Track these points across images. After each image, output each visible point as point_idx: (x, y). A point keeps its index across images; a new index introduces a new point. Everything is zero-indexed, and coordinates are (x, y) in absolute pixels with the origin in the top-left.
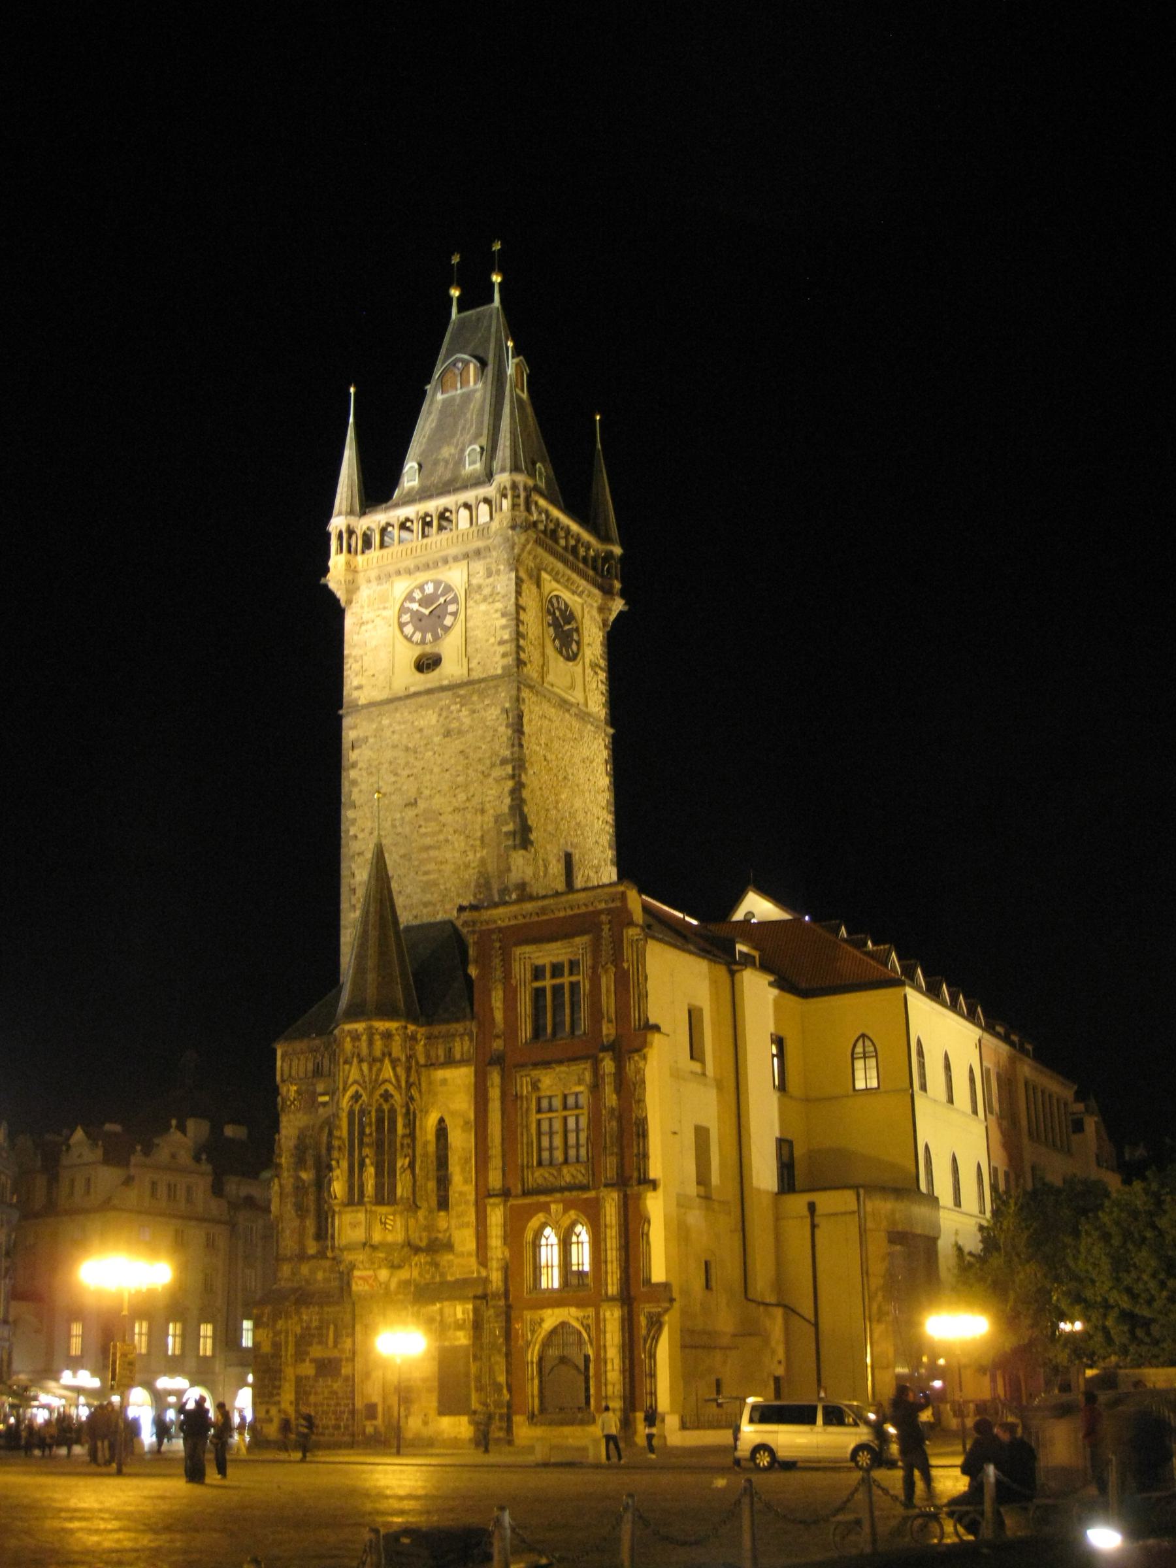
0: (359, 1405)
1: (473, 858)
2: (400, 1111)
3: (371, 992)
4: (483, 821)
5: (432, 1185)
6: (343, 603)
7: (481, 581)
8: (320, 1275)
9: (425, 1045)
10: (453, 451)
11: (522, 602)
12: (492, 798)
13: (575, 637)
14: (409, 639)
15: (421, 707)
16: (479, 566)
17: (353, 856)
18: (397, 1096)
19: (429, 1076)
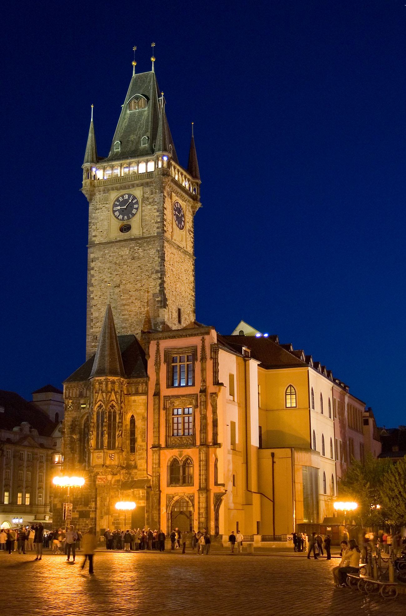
1: (144, 310)
2: (118, 412)
3: (107, 365)
4: (148, 296)
5: (128, 442)
6: (88, 200)
7: (148, 196)
9: (127, 386)
10: (135, 137)
11: (165, 206)
12: (152, 286)
13: (183, 220)
14: (117, 218)
16: (148, 189)
17: (92, 306)
18: (117, 407)
19: (128, 399)
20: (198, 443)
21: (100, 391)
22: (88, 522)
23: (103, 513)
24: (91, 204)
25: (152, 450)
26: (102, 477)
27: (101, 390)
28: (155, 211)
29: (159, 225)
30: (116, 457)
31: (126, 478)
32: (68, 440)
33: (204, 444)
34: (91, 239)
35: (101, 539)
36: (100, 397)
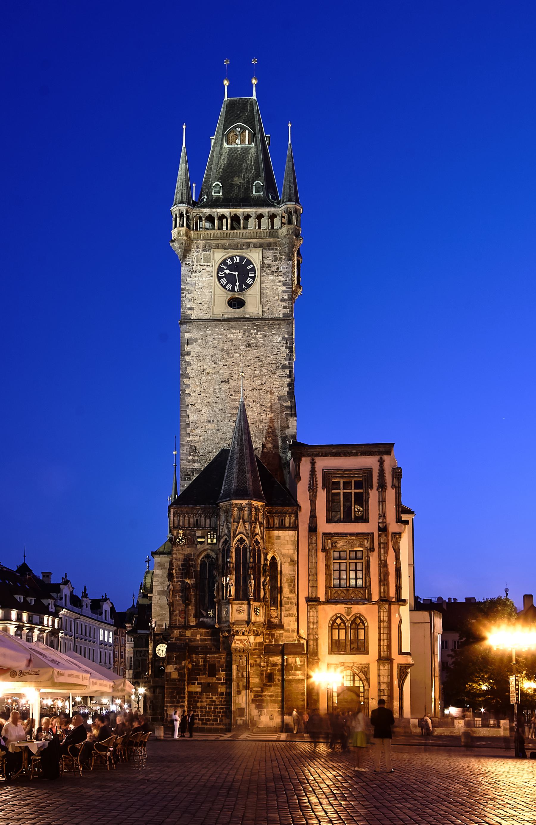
0: (234, 708)
7: (270, 262)
8: (198, 637)
10: (242, 181)
12: (277, 386)
14: (224, 287)
16: (269, 254)
20: (375, 597)
21: (241, 520)
22: (216, 698)
23: (241, 687)
24: (184, 263)
26: (242, 637)
27: (243, 519)
28: (281, 284)
29: (287, 304)
30: (262, 612)
31: (267, 641)
32: (179, 586)
33: (384, 600)
34: (185, 312)
35: (238, 721)
36: (240, 528)
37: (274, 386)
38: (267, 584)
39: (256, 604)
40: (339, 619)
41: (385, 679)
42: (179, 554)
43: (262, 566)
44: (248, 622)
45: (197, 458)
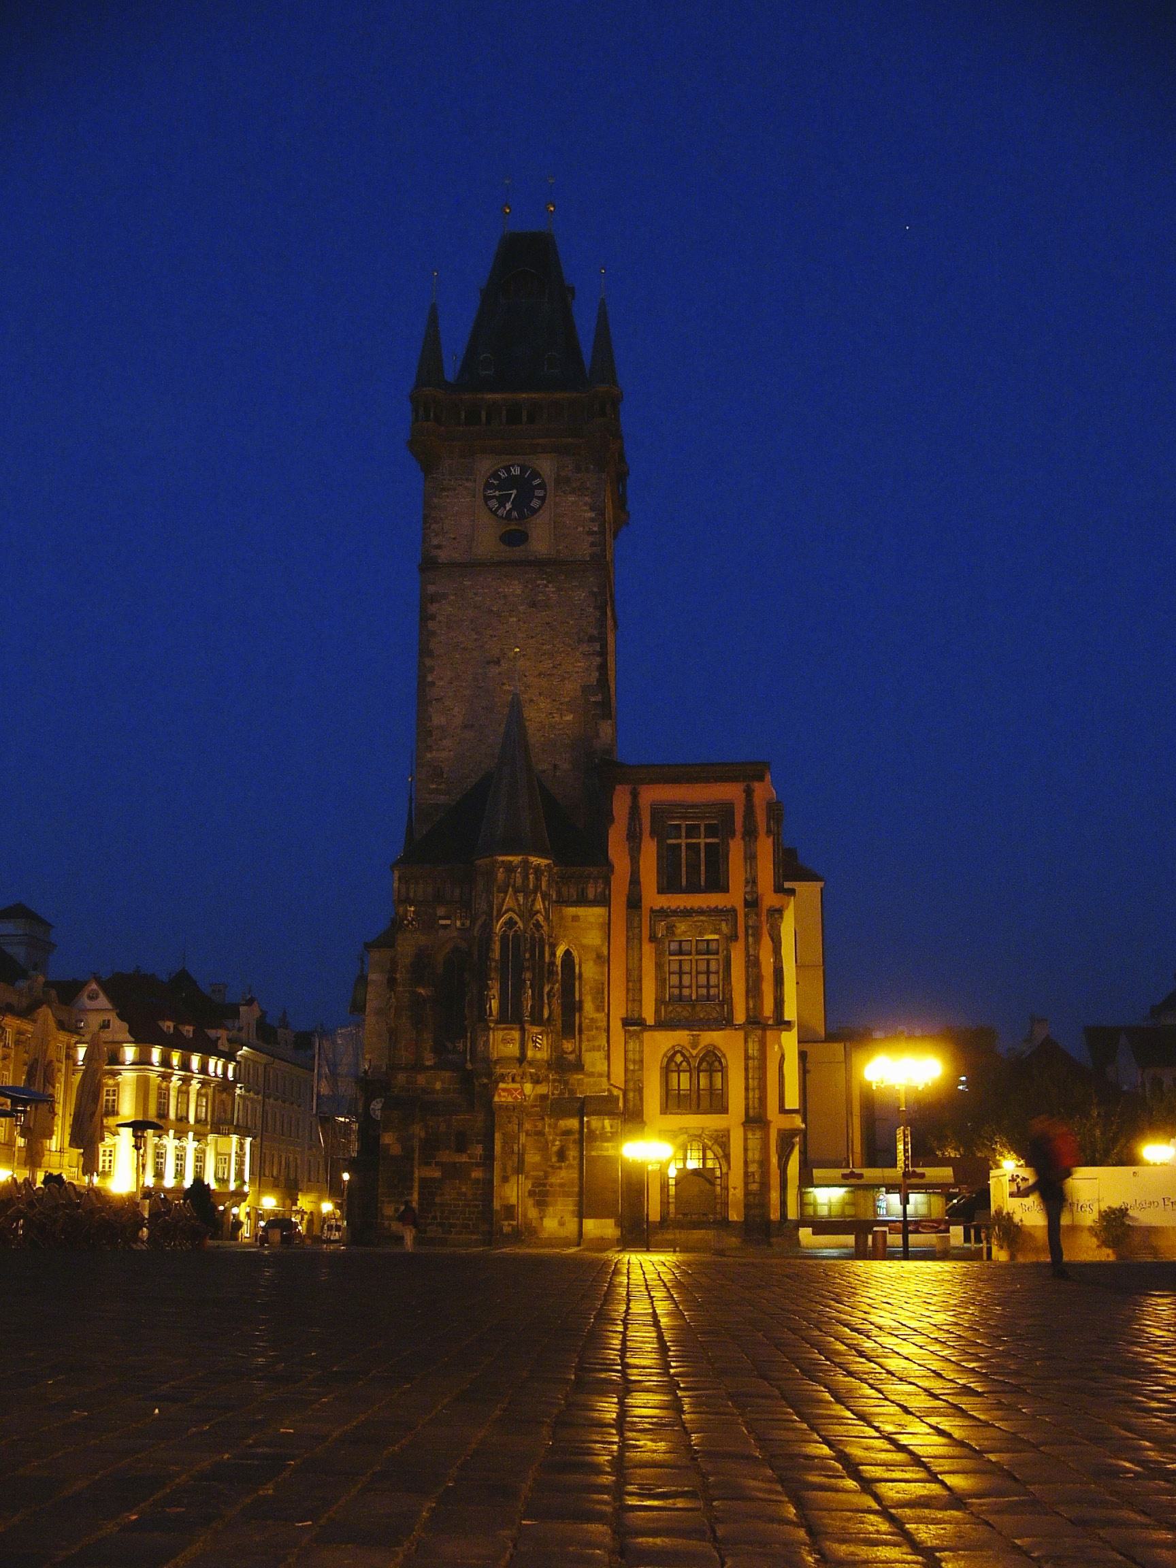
0: (497, 1205)
8: (438, 1086)
14: (495, 513)
15: (505, 576)
20: (740, 1017)
21: (510, 889)
25: (626, 1031)
27: (514, 886)
30: (545, 1042)
31: (556, 1092)
36: (509, 902)
37: (577, 669)
38: (554, 996)
39: (536, 1029)
40: (679, 1055)
41: (754, 1155)
42: (406, 947)
43: (546, 965)
44: (522, 1059)
45: (443, 786)
